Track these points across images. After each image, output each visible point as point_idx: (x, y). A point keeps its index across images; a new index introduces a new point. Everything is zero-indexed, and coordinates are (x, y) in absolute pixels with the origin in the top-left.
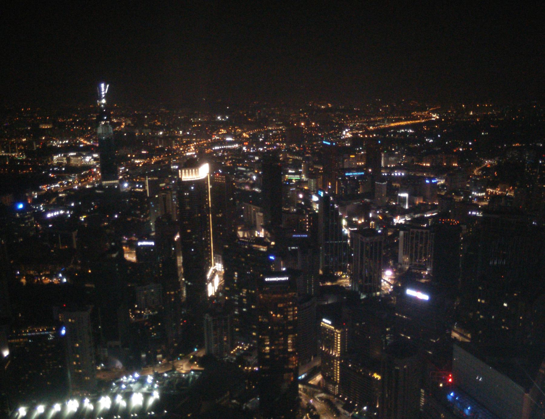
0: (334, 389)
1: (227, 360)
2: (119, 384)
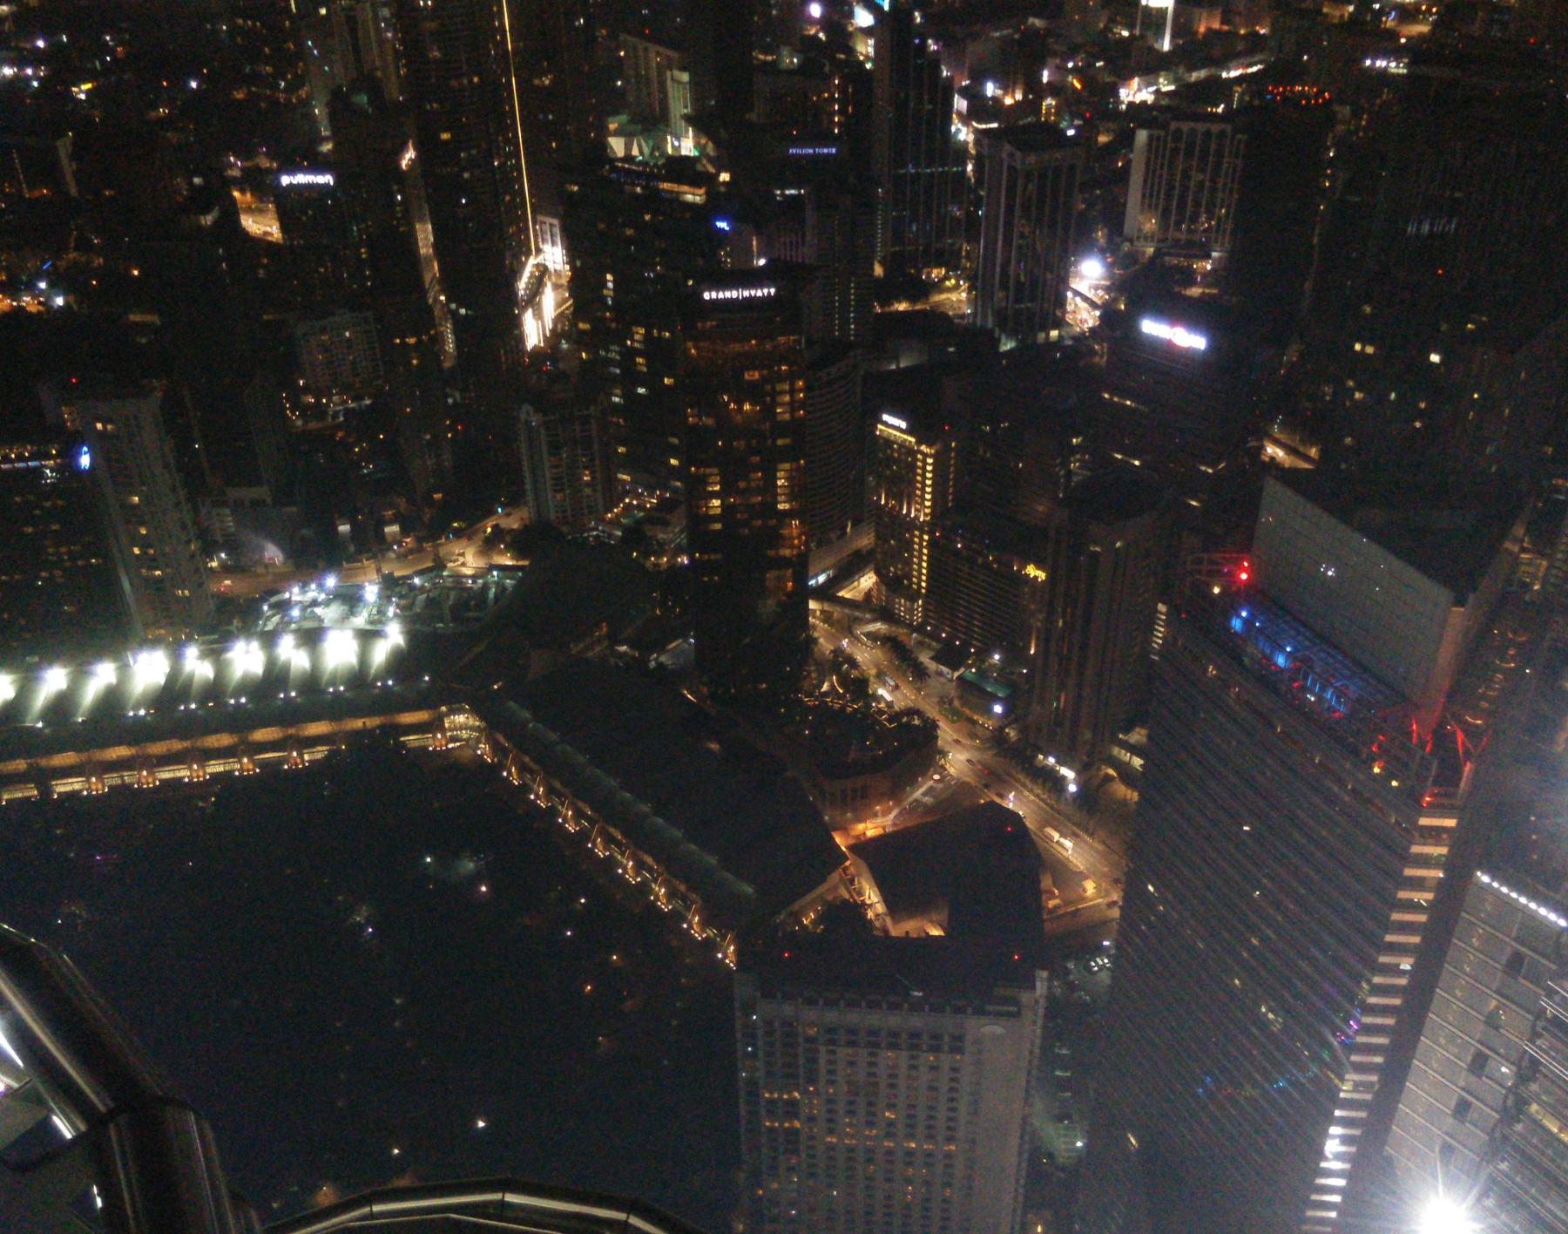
0: (911, 611)
1: (597, 537)
2: (283, 606)
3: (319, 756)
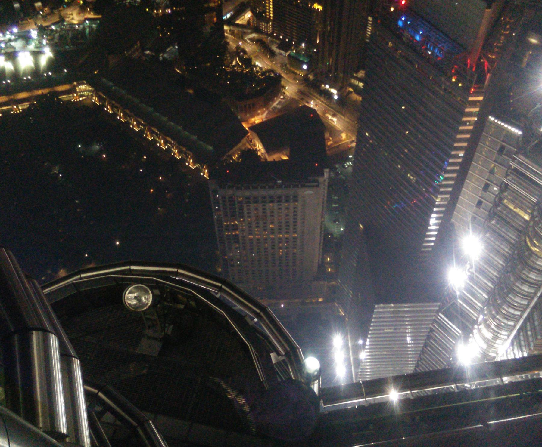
0: (267, 27)
3: (26, 107)
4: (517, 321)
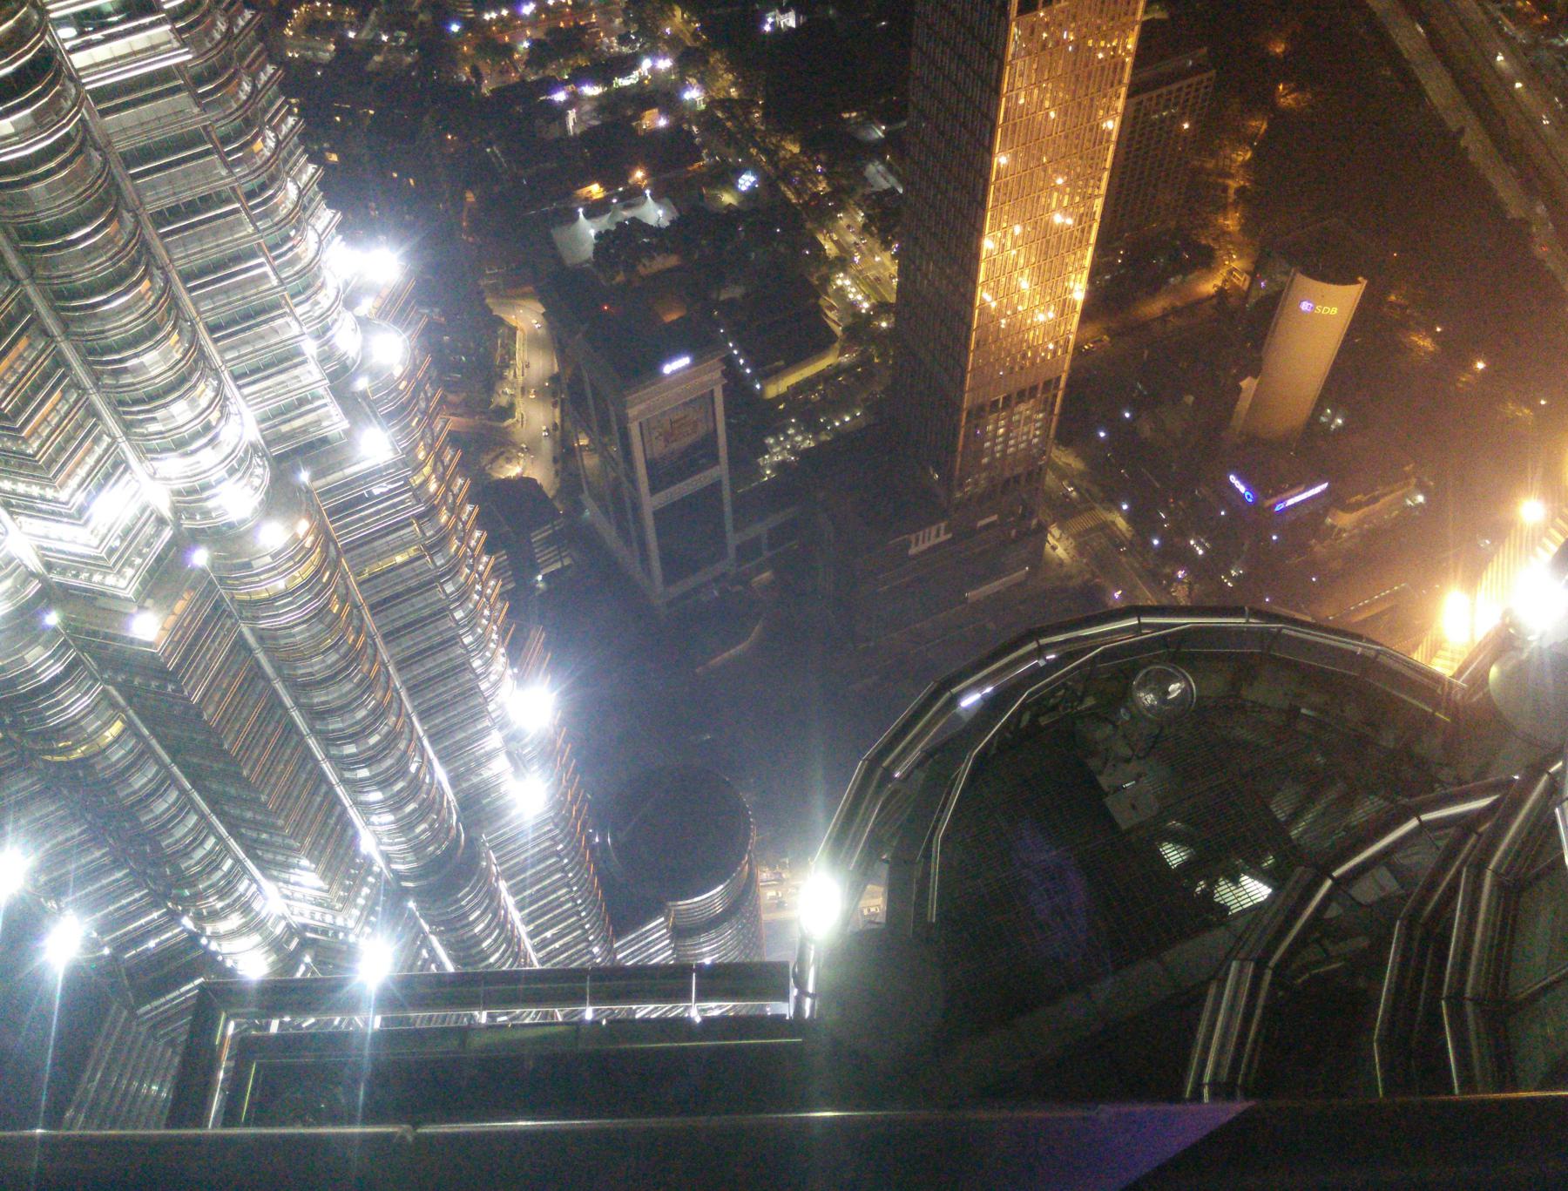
4: (228, 849)
